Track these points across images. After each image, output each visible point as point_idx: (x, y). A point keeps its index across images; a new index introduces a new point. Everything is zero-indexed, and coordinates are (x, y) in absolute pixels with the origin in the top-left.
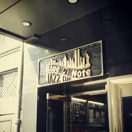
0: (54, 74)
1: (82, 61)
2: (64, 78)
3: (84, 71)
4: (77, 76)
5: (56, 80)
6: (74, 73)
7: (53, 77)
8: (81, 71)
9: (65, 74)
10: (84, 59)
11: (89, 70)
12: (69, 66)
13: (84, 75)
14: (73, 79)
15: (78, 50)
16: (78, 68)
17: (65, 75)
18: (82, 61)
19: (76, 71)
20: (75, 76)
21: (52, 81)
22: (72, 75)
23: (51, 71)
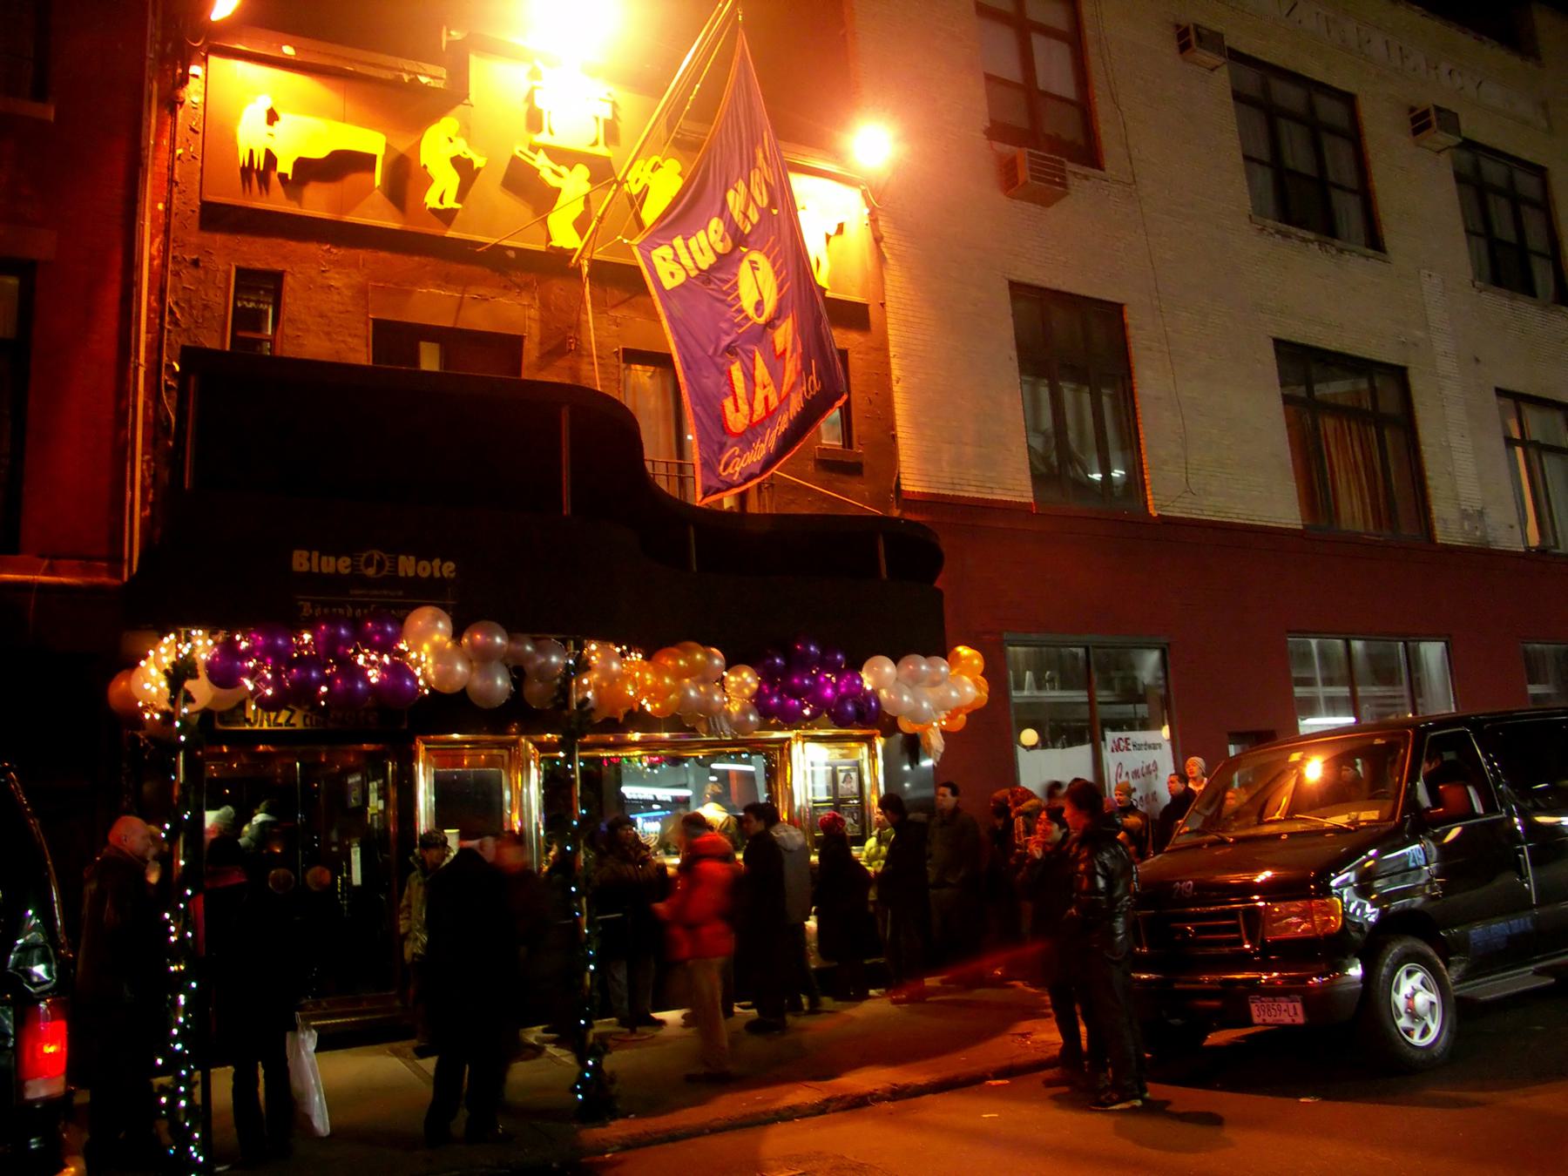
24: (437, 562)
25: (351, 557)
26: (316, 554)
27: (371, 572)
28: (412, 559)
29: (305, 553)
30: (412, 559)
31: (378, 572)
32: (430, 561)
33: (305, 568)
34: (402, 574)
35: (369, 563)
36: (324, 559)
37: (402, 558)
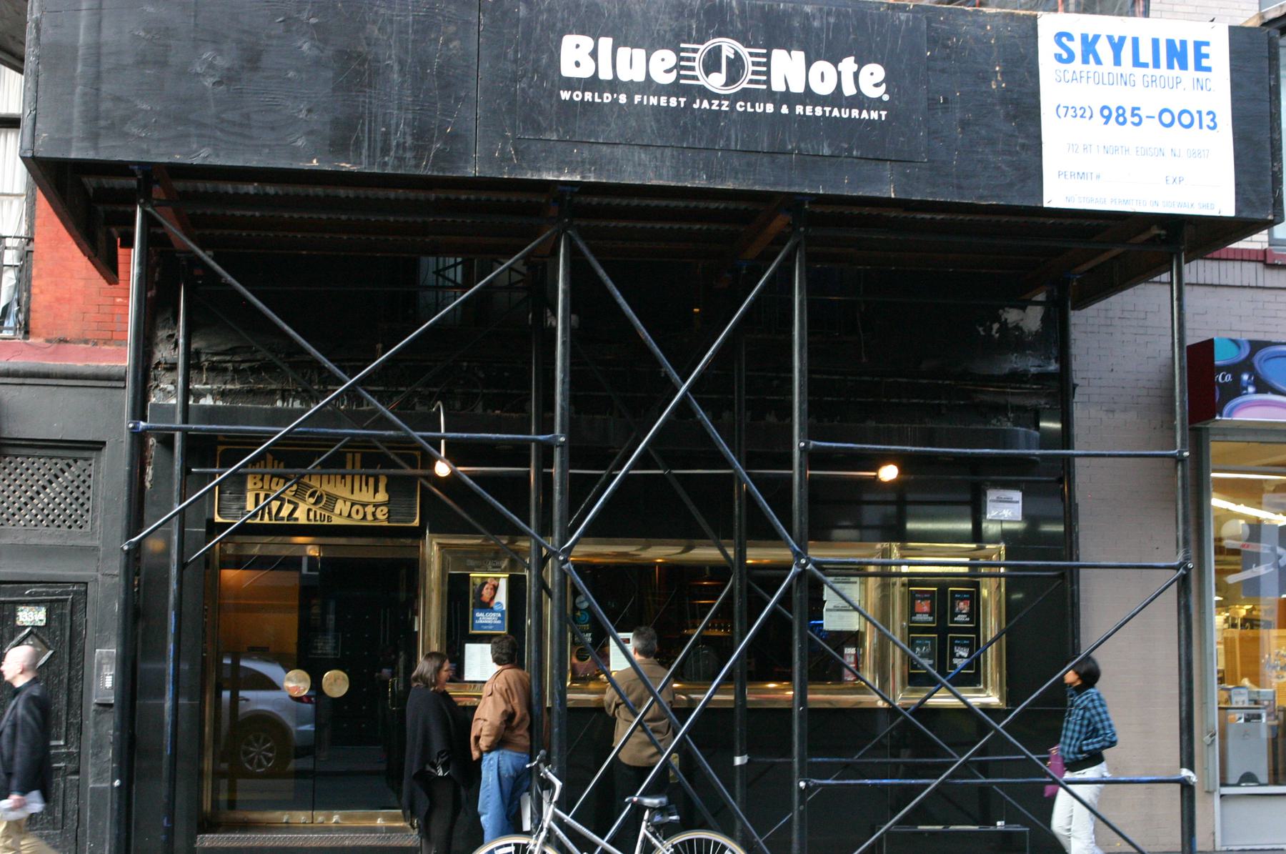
0: (276, 498)
1: (367, 484)
2: (312, 515)
3: (370, 509)
4: (349, 515)
5: (285, 512)
6: (340, 505)
7: (275, 505)
8: (364, 505)
9: (315, 504)
10: (371, 481)
11: (385, 509)
12: (327, 488)
13: (370, 517)
14: (336, 521)
15: (358, 457)
16: (357, 496)
17: (314, 508)
18: (367, 484)
19: (349, 504)
20: (345, 513)
21: (270, 513)
22: (337, 511)
23: (266, 487)
24: (848, 65)
25: (677, 51)
26: (606, 43)
27: (716, 82)
28: (799, 56)
29: (587, 42)
30: (799, 56)
31: (732, 79)
32: (835, 62)
33: (586, 72)
34: (778, 86)
35: (712, 64)
36: (624, 52)
37: (778, 55)
